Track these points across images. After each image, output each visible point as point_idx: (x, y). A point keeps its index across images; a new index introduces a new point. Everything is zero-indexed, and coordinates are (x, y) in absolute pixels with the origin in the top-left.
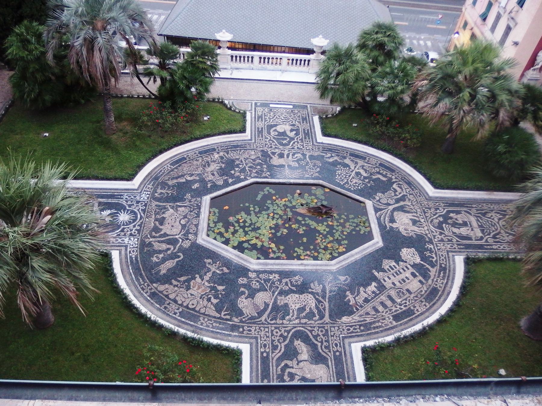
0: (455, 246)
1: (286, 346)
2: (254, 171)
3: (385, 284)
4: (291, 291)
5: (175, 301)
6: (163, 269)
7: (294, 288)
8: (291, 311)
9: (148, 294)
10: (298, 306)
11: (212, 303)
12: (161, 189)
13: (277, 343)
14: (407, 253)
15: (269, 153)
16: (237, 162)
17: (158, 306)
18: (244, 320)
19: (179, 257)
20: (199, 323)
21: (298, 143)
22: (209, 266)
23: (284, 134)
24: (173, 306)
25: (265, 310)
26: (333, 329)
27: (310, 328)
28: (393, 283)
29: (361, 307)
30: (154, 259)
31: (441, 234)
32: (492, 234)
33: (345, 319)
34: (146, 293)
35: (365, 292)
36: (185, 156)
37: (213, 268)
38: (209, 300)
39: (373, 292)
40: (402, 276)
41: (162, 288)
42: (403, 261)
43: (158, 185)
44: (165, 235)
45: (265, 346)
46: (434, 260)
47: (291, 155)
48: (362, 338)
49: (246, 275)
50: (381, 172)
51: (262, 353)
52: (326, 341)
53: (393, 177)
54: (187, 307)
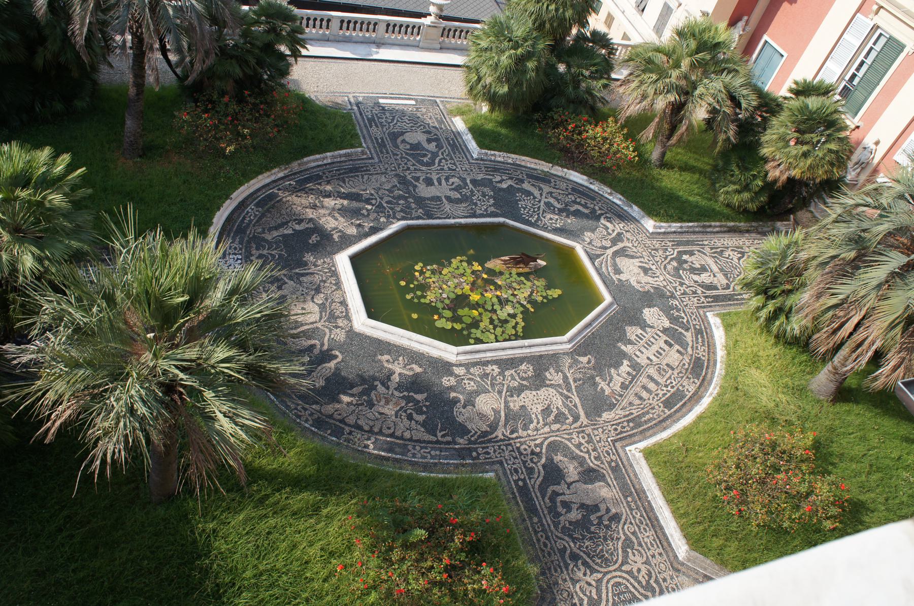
0: (703, 299)
3: (639, 360)
7: (525, 383)
8: (533, 416)
9: (311, 422)
10: (540, 408)
11: (417, 422)
20: (410, 454)
21: (447, 160)
26: (596, 432)
27: (567, 436)
28: (648, 358)
29: (621, 396)
31: (681, 284)
33: (606, 416)
35: (618, 375)
39: (628, 373)
43: (249, 242)
46: (685, 321)
50: (578, 200)
51: (516, 482)
52: (594, 450)
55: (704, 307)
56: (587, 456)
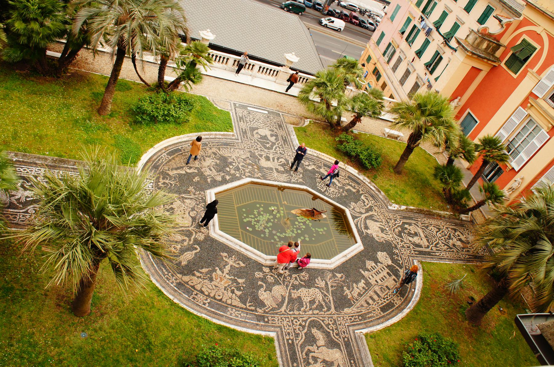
0: (413, 252)
1: (306, 334)
2: (247, 171)
3: (370, 281)
4: (302, 286)
5: (202, 292)
8: (304, 303)
9: (175, 284)
12: (163, 179)
13: (298, 332)
14: (382, 256)
15: (257, 154)
16: (230, 160)
17: (187, 296)
18: (267, 310)
19: (196, 249)
20: (228, 313)
21: (280, 148)
22: (226, 260)
23: (265, 137)
24: (201, 297)
26: (339, 319)
27: (321, 319)
28: (376, 281)
29: (357, 300)
31: (402, 241)
32: (434, 244)
33: (346, 310)
34: (172, 283)
35: (357, 288)
36: (180, 147)
37: (231, 262)
38: (233, 292)
39: (363, 288)
40: (381, 275)
41: (186, 278)
42: (380, 262)
45: (289, 334)
46: (401, 262)
47: (276, 160)
48: (361, 327)
49: (261, 270)
50: (351, 183)
51: (288, 340)
53: (360, 190)
55: (413, 257)
56: (331, 332)
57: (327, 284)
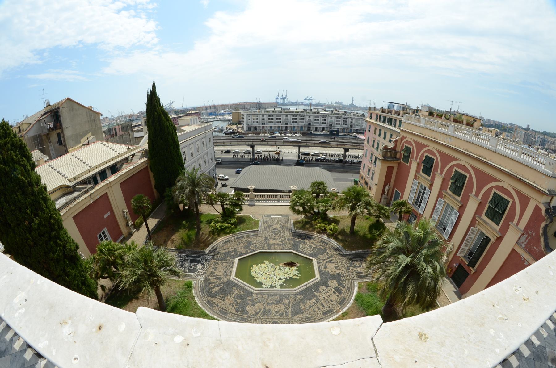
4: (273, 303)
5: (218, 306)
6: (214, 291)
24: (217, 308)
25: (259, 311)
30: (210, 286)
33: (298, 316)
37: (236, 292)
38: (233, 306)
40: (329, 294)
41: (212, 299)
44: (216, 275)
49: (251, 295)
54: (223, 308)
57: (290, 302)
